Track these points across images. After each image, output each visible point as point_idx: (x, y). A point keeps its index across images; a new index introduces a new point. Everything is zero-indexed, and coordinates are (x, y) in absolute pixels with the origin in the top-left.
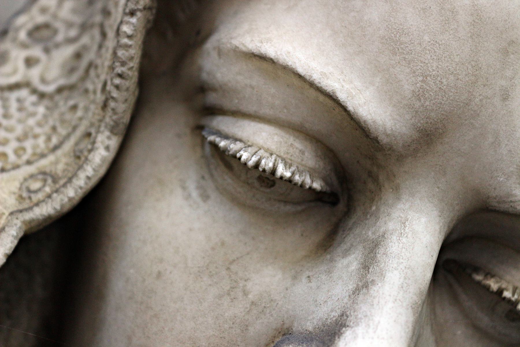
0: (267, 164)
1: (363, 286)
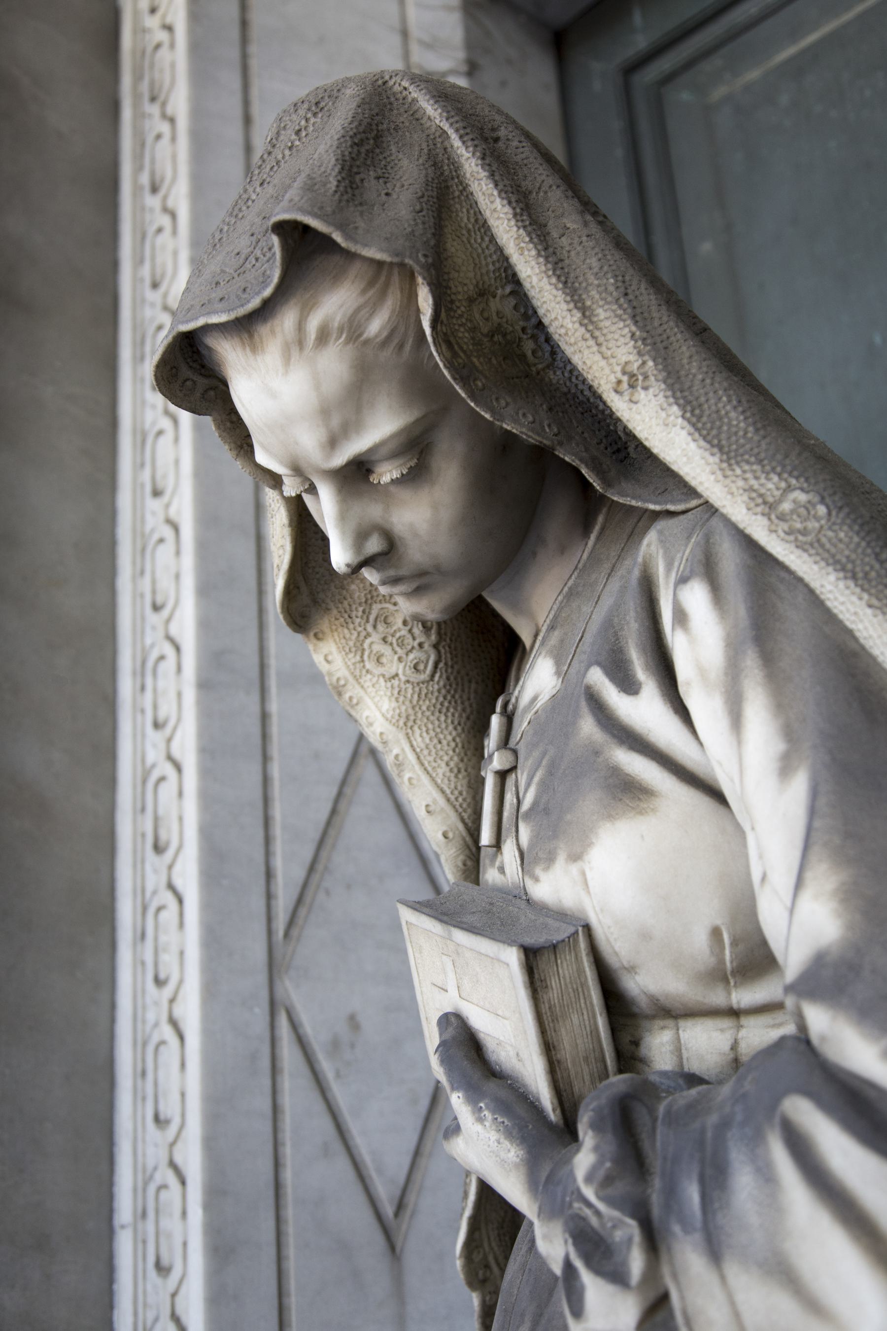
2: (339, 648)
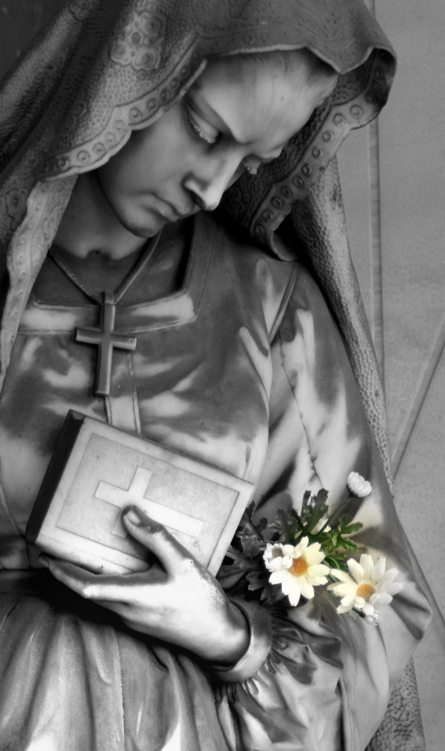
0: (206, 138)
1: (218, 173)
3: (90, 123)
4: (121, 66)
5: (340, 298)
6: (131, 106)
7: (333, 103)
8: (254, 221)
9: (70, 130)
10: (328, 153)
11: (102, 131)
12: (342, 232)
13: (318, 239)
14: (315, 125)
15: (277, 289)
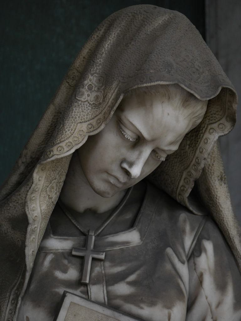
1: (138, 158)
2: (46, 177)
3: (64, 132)
4: (82, 102)
5: (229, 234)
6: (88, 123)
7: (209, 123)
8: (178, 193)
9: (54, 136)
10: (207, 150)
11: (71, 136)
12: (227, 197)
13: (214, 201)
14: (200, 136)
15: (192, 229)
